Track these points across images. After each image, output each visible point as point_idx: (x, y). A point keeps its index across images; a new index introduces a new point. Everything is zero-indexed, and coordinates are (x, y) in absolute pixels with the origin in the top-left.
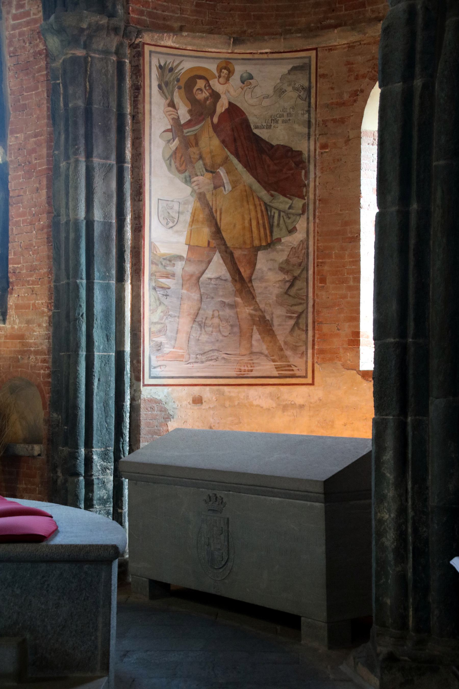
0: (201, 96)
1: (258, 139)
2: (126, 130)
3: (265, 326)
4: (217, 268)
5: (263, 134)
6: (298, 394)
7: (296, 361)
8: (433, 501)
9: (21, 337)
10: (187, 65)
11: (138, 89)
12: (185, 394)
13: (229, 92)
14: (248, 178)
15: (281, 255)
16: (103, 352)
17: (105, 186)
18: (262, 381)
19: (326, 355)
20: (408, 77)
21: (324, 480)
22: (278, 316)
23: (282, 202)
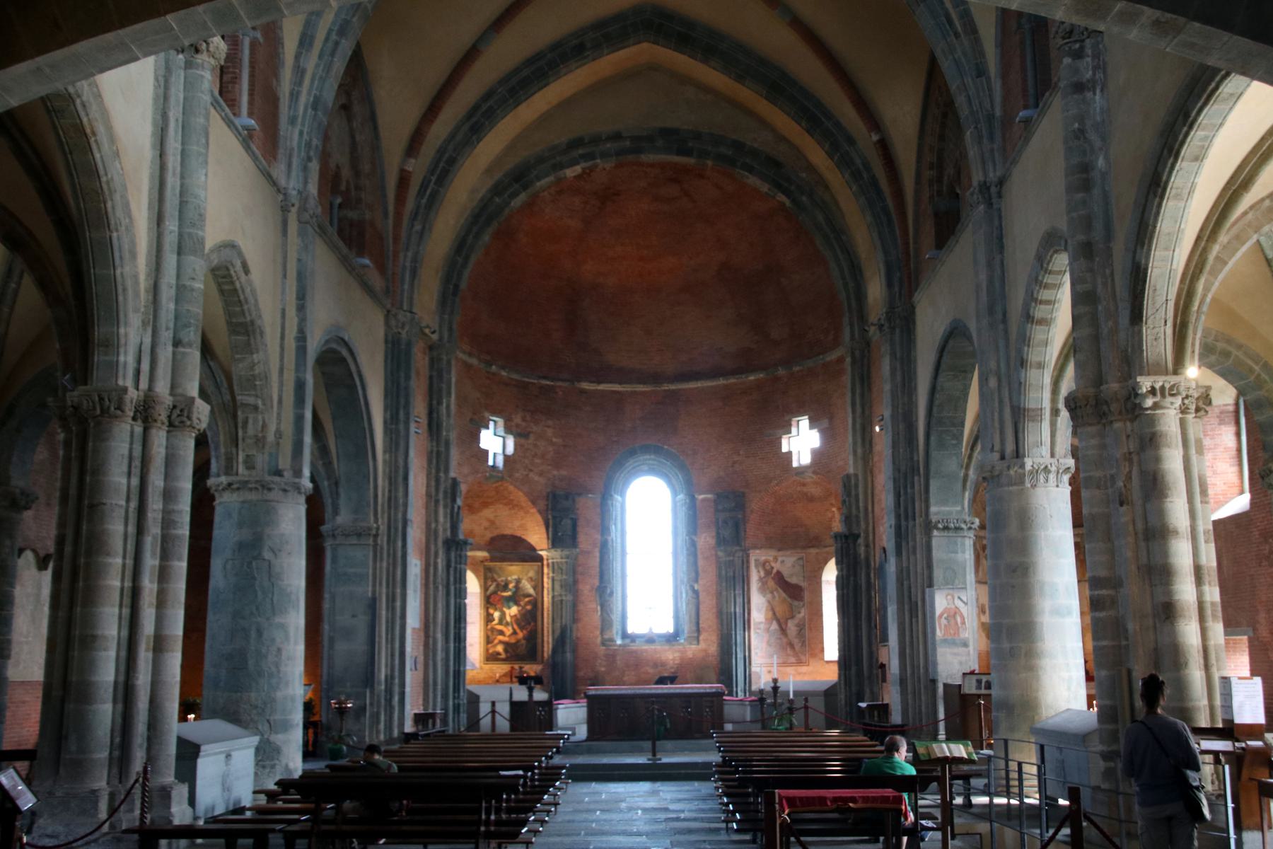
2: (745, 581)
3: (792, 646)
4: (775, 626)
5: (788, 580)
6: (804, 669)
7: (803, 657)
8: (854, 689)
9: (705, 651)
11: (748, 567)
12: (764, 669)
13: (777, 566)
15: (796, 621)
16: (740, 655)
17: (739, 600)
18: (791, 665)
19: (813, 655)
21: (826, 687)
22: (796, 641)
23: (796, 603)
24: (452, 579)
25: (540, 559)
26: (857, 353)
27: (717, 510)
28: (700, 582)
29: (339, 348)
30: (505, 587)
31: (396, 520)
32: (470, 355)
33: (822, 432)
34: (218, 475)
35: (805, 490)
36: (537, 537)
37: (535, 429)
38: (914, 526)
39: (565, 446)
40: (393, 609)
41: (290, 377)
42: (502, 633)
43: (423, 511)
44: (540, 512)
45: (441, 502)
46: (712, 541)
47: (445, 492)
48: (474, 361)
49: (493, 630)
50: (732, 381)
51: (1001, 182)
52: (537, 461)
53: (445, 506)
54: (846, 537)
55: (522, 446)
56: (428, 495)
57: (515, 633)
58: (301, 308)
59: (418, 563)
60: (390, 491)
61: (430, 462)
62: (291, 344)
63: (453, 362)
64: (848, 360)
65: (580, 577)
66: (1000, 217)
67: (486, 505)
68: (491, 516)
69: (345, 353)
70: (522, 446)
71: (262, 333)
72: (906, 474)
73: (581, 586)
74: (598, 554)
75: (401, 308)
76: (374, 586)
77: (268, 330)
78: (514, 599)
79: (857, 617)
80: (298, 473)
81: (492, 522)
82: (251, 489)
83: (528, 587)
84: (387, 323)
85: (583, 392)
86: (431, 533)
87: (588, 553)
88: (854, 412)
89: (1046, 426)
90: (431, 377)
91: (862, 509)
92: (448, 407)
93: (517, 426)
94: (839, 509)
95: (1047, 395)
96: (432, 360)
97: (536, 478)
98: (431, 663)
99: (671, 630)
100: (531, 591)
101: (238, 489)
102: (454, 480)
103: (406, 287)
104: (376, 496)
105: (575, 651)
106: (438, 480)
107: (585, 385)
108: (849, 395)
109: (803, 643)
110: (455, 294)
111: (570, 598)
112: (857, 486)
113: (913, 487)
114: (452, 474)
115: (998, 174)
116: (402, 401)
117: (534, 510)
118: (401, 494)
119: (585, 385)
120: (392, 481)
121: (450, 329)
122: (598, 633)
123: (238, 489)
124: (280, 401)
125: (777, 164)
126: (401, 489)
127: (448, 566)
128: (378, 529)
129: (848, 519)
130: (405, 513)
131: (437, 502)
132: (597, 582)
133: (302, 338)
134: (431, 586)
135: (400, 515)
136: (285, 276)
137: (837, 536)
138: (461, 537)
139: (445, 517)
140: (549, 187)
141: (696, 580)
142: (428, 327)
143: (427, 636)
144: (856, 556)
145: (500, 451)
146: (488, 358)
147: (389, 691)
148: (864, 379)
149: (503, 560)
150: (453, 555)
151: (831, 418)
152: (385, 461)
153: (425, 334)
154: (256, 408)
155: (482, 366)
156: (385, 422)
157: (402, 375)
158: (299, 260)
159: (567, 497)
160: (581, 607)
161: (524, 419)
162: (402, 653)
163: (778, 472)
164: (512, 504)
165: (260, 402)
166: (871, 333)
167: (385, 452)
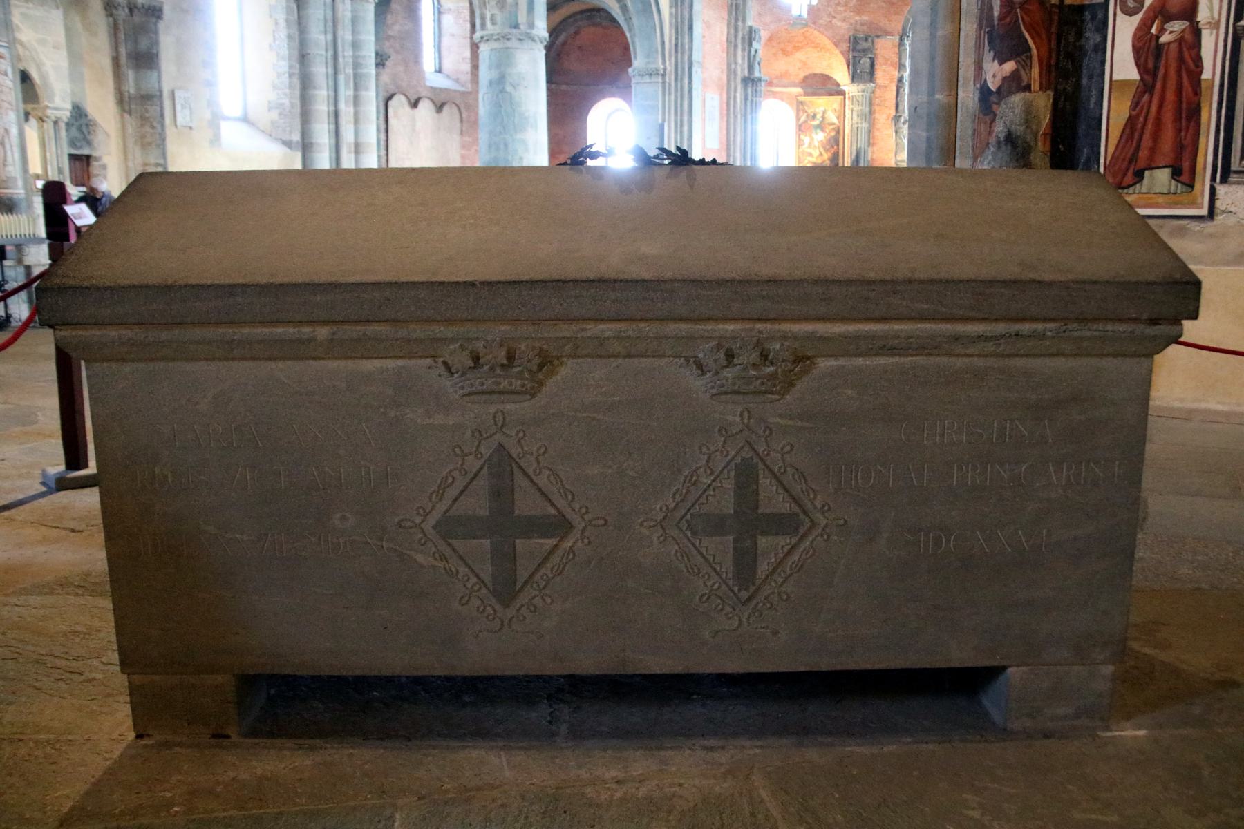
25: (842, 93)
30: (814, 117)
31: (683, 62)
36: (841, 74)
42: (810, 155)
43: (725, 55)
44: (842, 53)
45: (740, 46)
47: (743, 38)
49: (803, 152)
53: (743, 50)
56: (728, 40)
57: (821, 155)
59: (717, 97)
61: (730, 13)
65: (876, 108)
67: (797, 48)
68: (803, 58)
73: (877, 116)
78: (821, 127)
81: (805, 64)
83: (832, 118)
86: (731, 73)
97: (839, 24)
100: (835, 120)
102: (751, 27)
104: (663, 43)
106: (736, 30)
111: (865, 125)
114: (749, 23)
117: (837, 52)
118: (686, 41)
120: (677, 30)
127: (746, 99)
128: (665, 69)
130: (690, 56)
131: (736, 46)
132: (893, 113)
135: (686, 58)
138: (757, 74)
139: (743, 58)
149: (814, 94)
150: (749, 90)
152: (671, 14)
159: (866, 40)
160: (877, 133)
164: (817, 46)
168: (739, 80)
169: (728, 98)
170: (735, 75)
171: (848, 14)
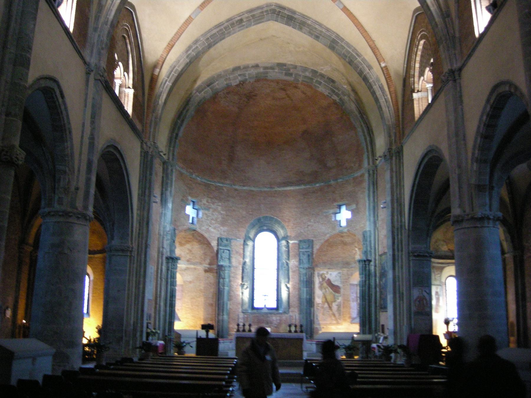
0: (324, 277)
1: (332, 284)
3: (334, 315)
4: (326, 305)
7: (339, 321)
10: (321, 272)
13: (328, 276)
14: (331, 291)
15: (336, 303)
18: (334, 324)
20: (362, 287)
23: (337, 294)
24: (169, 276)
26: (371, 172)
27: (299, 248)
28: (290, 283)
29: (115, 153)
32: (182, 168)
33: (353, 211)
34: (44, 208)
35: (342, 239)
37: (213, 206)
38: (402, 255)
39: (227, 215)
40: (139, 288)
41: (85, 158)
46: (297, 264)
48: (184, 171)
50: (308, 186)
51: (460, 70)
52: (213, 222)
54: (365, 261)
55: (206, 214)
58: (93, 123)
60: (139, 230)
62: (86, 140)
63: (174, 171)
64: (366, 175)
65: (232, 279)
66: (460, 87)
69: (118, 156)
70: (206, 214)
71: (70, 132)
72: (398, 229)
73: (232, 283)
74: (241, 268)
75: (149, 139)
76: (129, 276)
77: (74, 132)
79: (370, 301)
80: (86, 208)
82: (60, 216)
84: (142, 147)
85: (236, 190)
87: (236, 267)
88: (369, 200)
89: (487, 193)
90: (163, 177)
91: (373, 248)
92: (171, 191)
93: (204, 204)
94: (359, 249)
95: (488, 177)
96: (163, 169)
97: (212, 230)
98: (157, 317)
99: (274, 306)
101: (53, 215)
103: (152, 130)
105: (228, 314)
107: (237, 187)
108: (367, 192)
109: (340, 314)
110: (176, 138)
112: (370, 236)
113: (401, 235)
115: (459, 65)
116: (148, 185)
118: (145, 231)
119: (237, 187)
120: (140, 223)
121: (173, 155)
122: (240, 306)
123: (53, 215)
124: (79, 171)
125: (333, 81)
126: (145, 229)
127: (168, 270)
128: (132, 248)
129: (365, 253)
130: (147, 241)
133: (92, 138)
134: (159, 279)
135: (144, 242)
136: (85, 106)
137: (359, 261)
140: (223, 90)
141: (288, 282)
142: (162, 152)
143: (156, 303)
144: (369, 270)
145: (195, 216)
146: (191, 171)
147: (135, 330)
148: (374, 184)
151: (357, 205)
152: (137, 214)
153: (161, 155)
154: (65, 172)
155: (188, 174)
156: (139, 195)
157: (148, 173)
158: (93, 98)
161: (207, 202)
162: (143, 311)
163: (330, 230)
165: (67, 169)
166: (378, 162)
167: (138, 210)
168: (164, 258)
169: (158, 268)
170: (162, 254)
171: (217, 225)
